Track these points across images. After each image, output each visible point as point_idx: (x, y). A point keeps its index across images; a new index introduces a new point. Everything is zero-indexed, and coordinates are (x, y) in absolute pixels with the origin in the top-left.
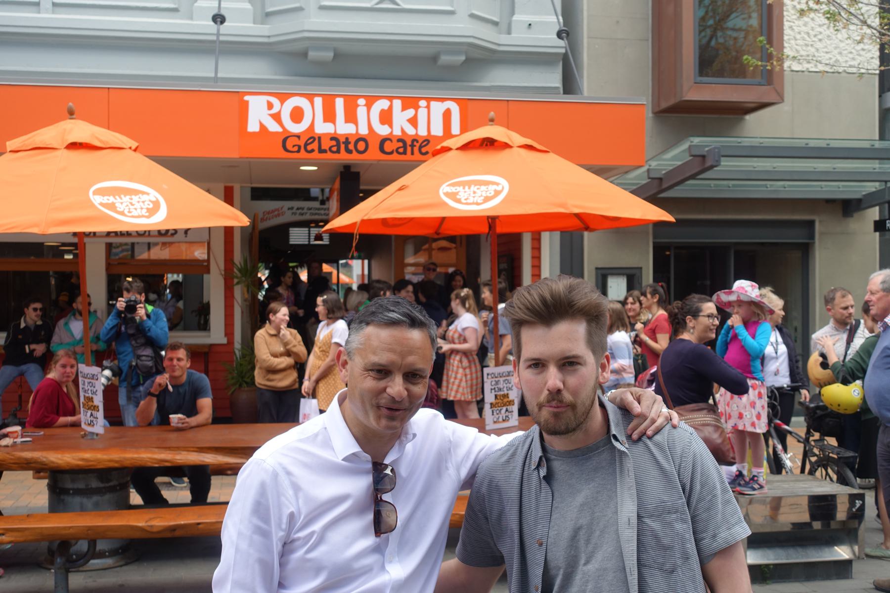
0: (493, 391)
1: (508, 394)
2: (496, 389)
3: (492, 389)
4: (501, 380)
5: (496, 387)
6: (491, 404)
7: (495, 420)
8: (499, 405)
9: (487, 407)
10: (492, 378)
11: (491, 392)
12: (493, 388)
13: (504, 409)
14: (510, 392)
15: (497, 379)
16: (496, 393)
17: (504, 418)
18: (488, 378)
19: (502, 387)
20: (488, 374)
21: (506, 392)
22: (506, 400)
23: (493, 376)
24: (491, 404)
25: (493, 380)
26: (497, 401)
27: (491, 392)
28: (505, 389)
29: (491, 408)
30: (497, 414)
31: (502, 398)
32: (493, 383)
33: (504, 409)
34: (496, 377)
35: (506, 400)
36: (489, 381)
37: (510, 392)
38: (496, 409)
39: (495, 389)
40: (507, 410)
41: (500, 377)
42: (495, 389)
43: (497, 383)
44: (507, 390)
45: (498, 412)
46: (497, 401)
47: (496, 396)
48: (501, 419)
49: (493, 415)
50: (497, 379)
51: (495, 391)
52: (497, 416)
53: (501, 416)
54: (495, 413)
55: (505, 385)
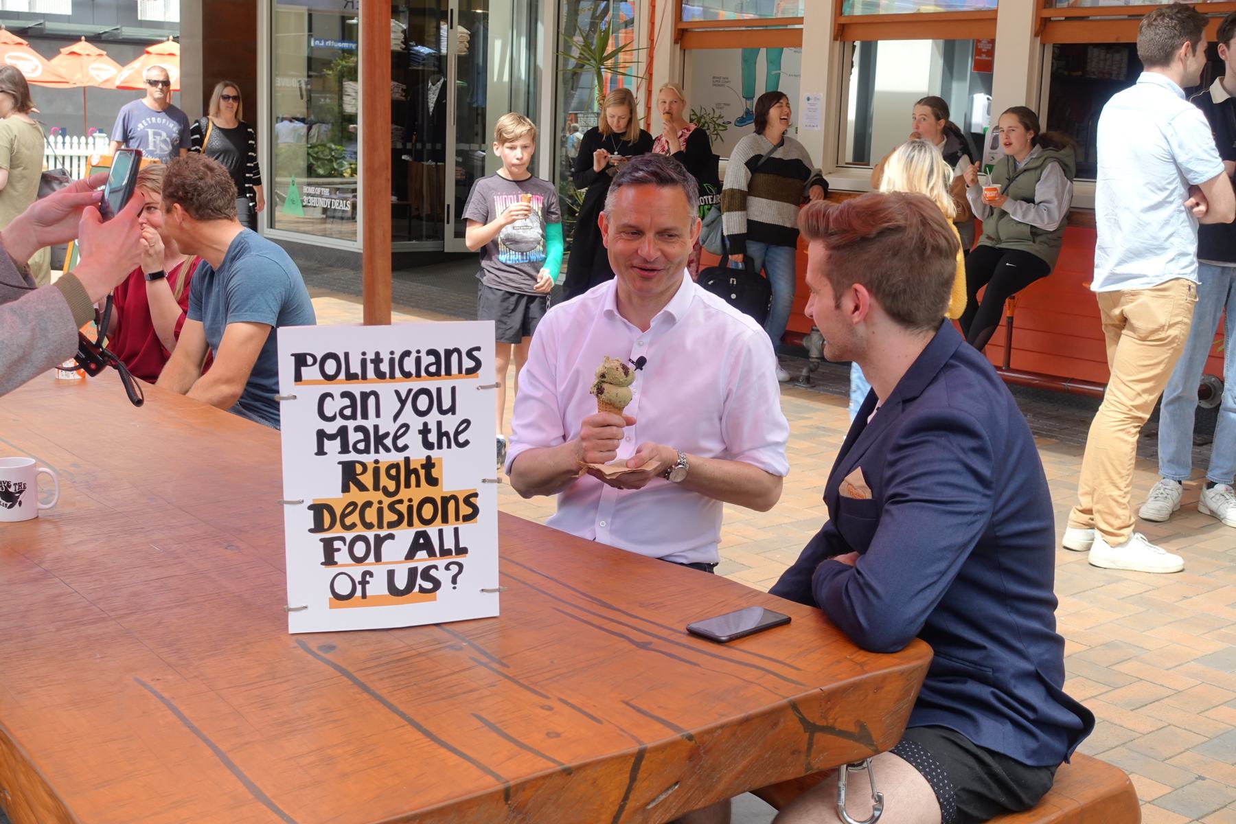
0: (333, 446)
1: (429, 464)
2: (354, 437)
3: (321, 435)
4: (386, 391)
5: (351, 424)
6: (318, 509)
7: (343, 587)
8: (371, 515)
9: (298, 521)
10: (329, 378)
11: (321, 451)
12: (331, 428)
13: (405, 536)
14: (446, 457)
15: (357, 388)
16: (352, 456)
17: (401, 583)
18: (298, 378)
19: (387, 425)
20: (300, 360)
21: (417, 454)
22: (414, 494)
23: (331, 367)
24: (318, 509)
25: (336, 388)
26: (358, 497)
27: (321, 451)
28: (413, 439)
29: (318, 527)
30: (359, 561)
31: (384, 481)
32: (331, 408)
33: (405, 536)
34: (351, 377)
35: (414, 494)
36: (308, 395)
37: (446, 457)
38: (349, 536)
39: (343, 432)
40: (421, 543)
41: (380, 375)
42: (343, 432)
43: (358, 405)
44: (428, 445)
45: (360, 549)
46: (358, 497)
47: (350, 474)
48: (378, 586)
49: (329, 560)
50: (357, 388)
51: (345, 449)
52: (357, 572)
53: (380, 573)
54: (342, 556)
55: (416, 423)
